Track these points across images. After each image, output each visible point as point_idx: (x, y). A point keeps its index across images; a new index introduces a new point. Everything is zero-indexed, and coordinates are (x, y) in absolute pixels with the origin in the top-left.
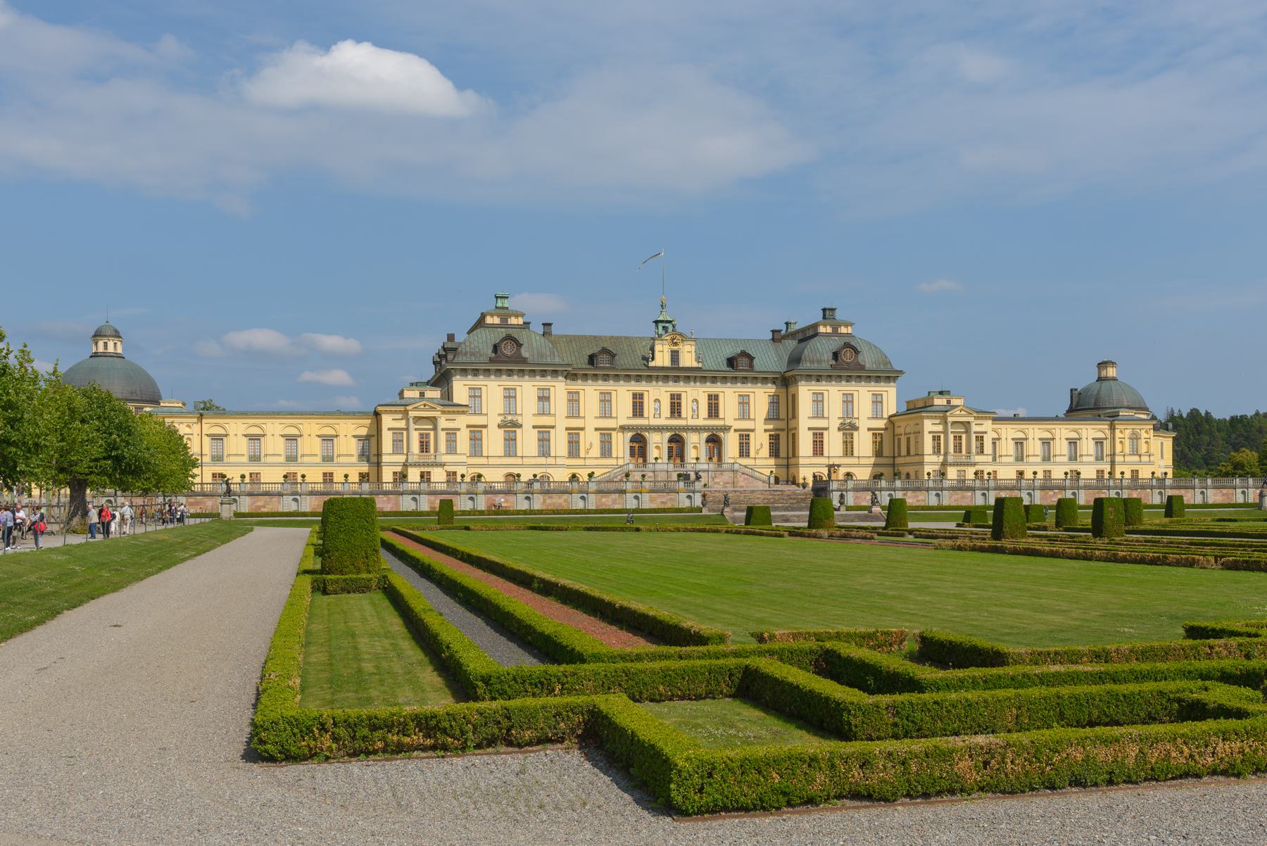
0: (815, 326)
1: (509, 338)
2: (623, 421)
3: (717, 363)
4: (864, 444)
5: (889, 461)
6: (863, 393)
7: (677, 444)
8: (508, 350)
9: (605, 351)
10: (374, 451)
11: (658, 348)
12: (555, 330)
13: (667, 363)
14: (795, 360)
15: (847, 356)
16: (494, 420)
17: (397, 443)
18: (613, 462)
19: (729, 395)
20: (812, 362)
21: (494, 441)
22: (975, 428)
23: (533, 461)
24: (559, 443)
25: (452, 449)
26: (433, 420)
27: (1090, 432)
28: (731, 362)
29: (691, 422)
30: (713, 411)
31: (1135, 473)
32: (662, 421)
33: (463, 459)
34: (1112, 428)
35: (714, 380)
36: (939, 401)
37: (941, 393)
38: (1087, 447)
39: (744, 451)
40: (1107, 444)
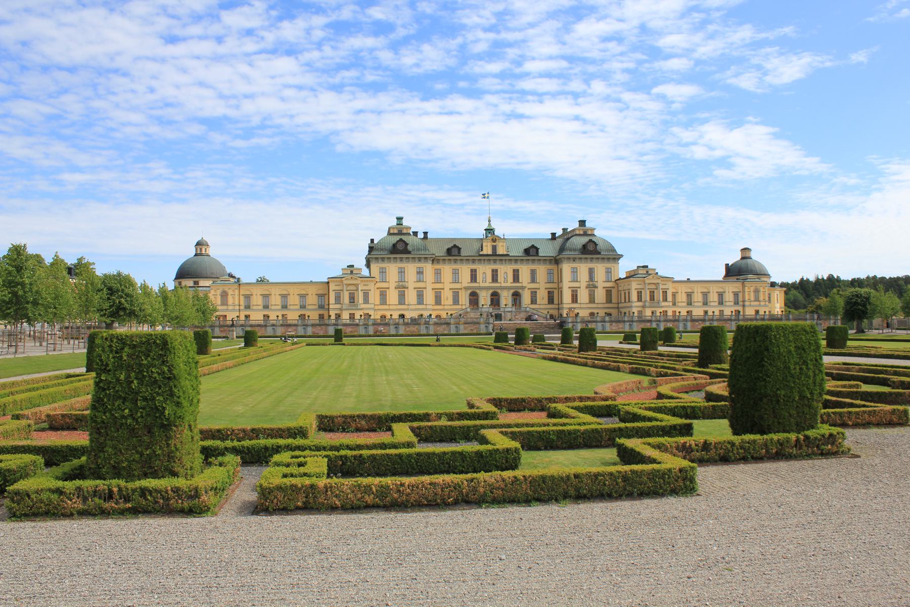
0: (574, 230)
1: (401, 240)
2: (467, 285)
3: (517, 252)
5: (616, 306)
6: (600, 269)
7: (495, 299)
8: (400, 247)
9: (455, 246)
11: (484, 244)
12: (429, 236)
13: (490, 252)
14: (562, 249)
15: (591, 247)
16: (392, 285)
17: (338, 299)
18: (459, 307)
19: (525, 271)
20: (571, 250)
21: (393, 297)
22: (661, 287)
23: (414, 307)
24: (429, 297)
25: (366, 300)
26: (357, 285)
27: (731, 288)
28: (527, 251)
29: (503, 285)
30: (516, 278)
31: (757, 312)
33: (372, 306)
34: (744, 286)
35: (516, 261)
36: (641, 271)
37: (644, 267)
38: (729, 297)
39: (534, 301)
40: (740, 295)
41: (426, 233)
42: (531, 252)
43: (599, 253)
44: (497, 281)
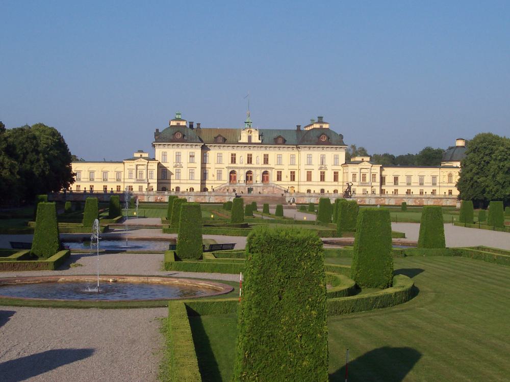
4: (329, 176)
7: (249, 176)
9: (220, 136)
10: (123, 177)
12: (201, 127)
19: (273, 154)
20: (307, 141)
30: (266, 161)
32: (243, 165)
39: (279, 178)
40: (438, 178)
41: (199, 124)
43: (330, 144)
44: (251, 163)
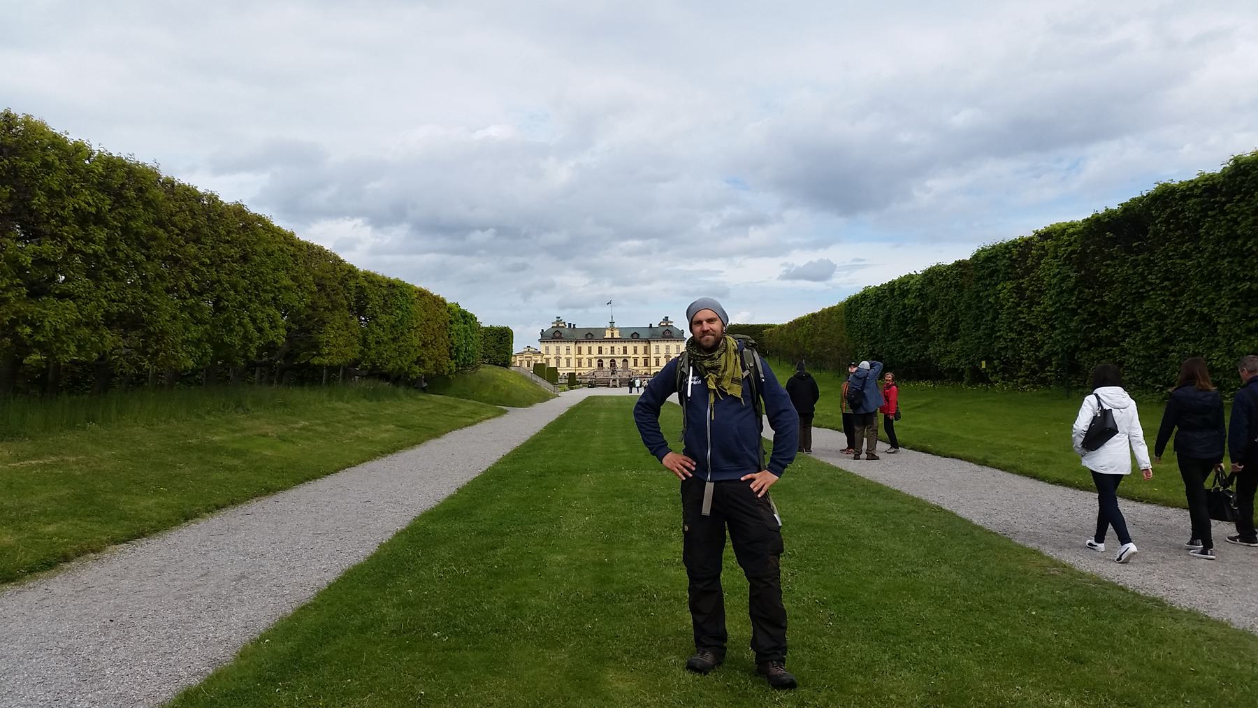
3: (627, 335)
19: (630, 347)
30: (625, 351)
39: (636, 364)
42: (635, 336)
